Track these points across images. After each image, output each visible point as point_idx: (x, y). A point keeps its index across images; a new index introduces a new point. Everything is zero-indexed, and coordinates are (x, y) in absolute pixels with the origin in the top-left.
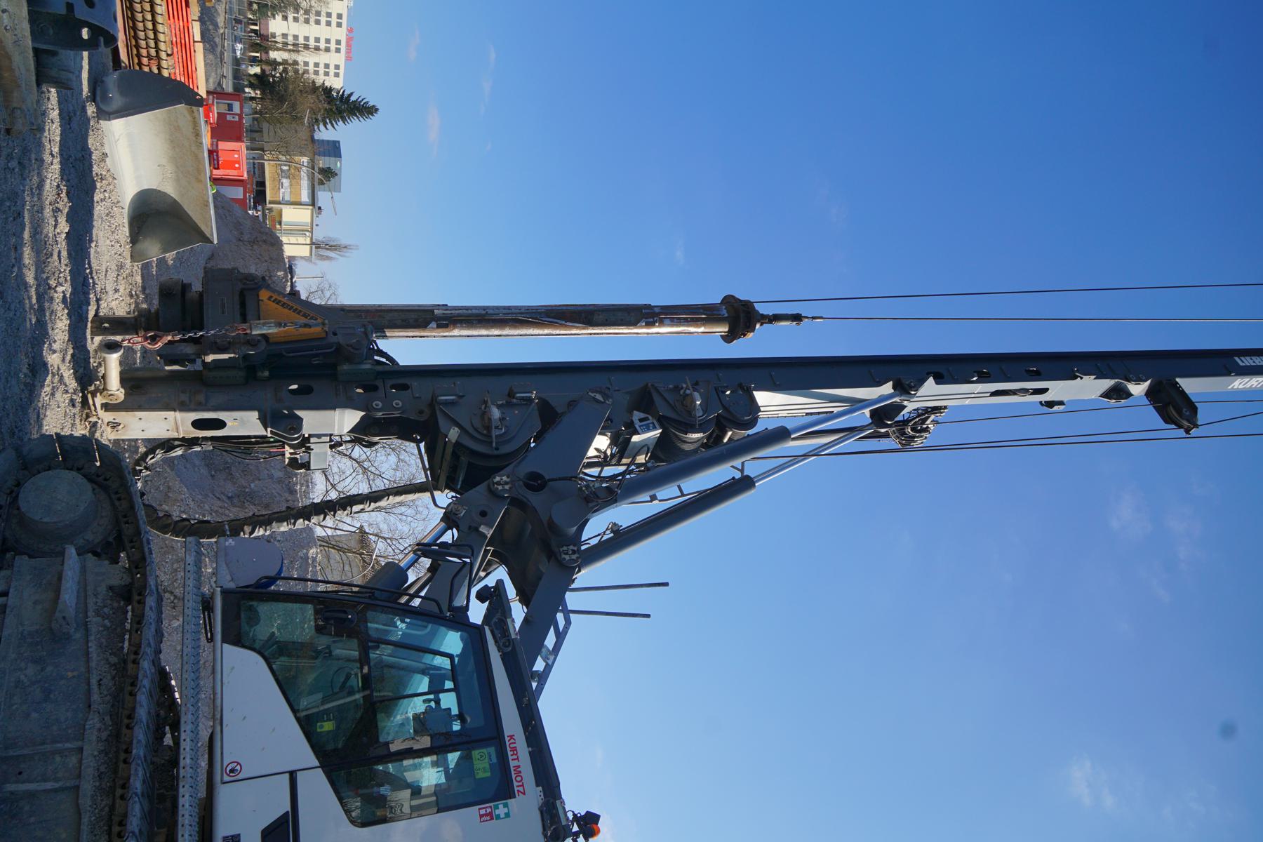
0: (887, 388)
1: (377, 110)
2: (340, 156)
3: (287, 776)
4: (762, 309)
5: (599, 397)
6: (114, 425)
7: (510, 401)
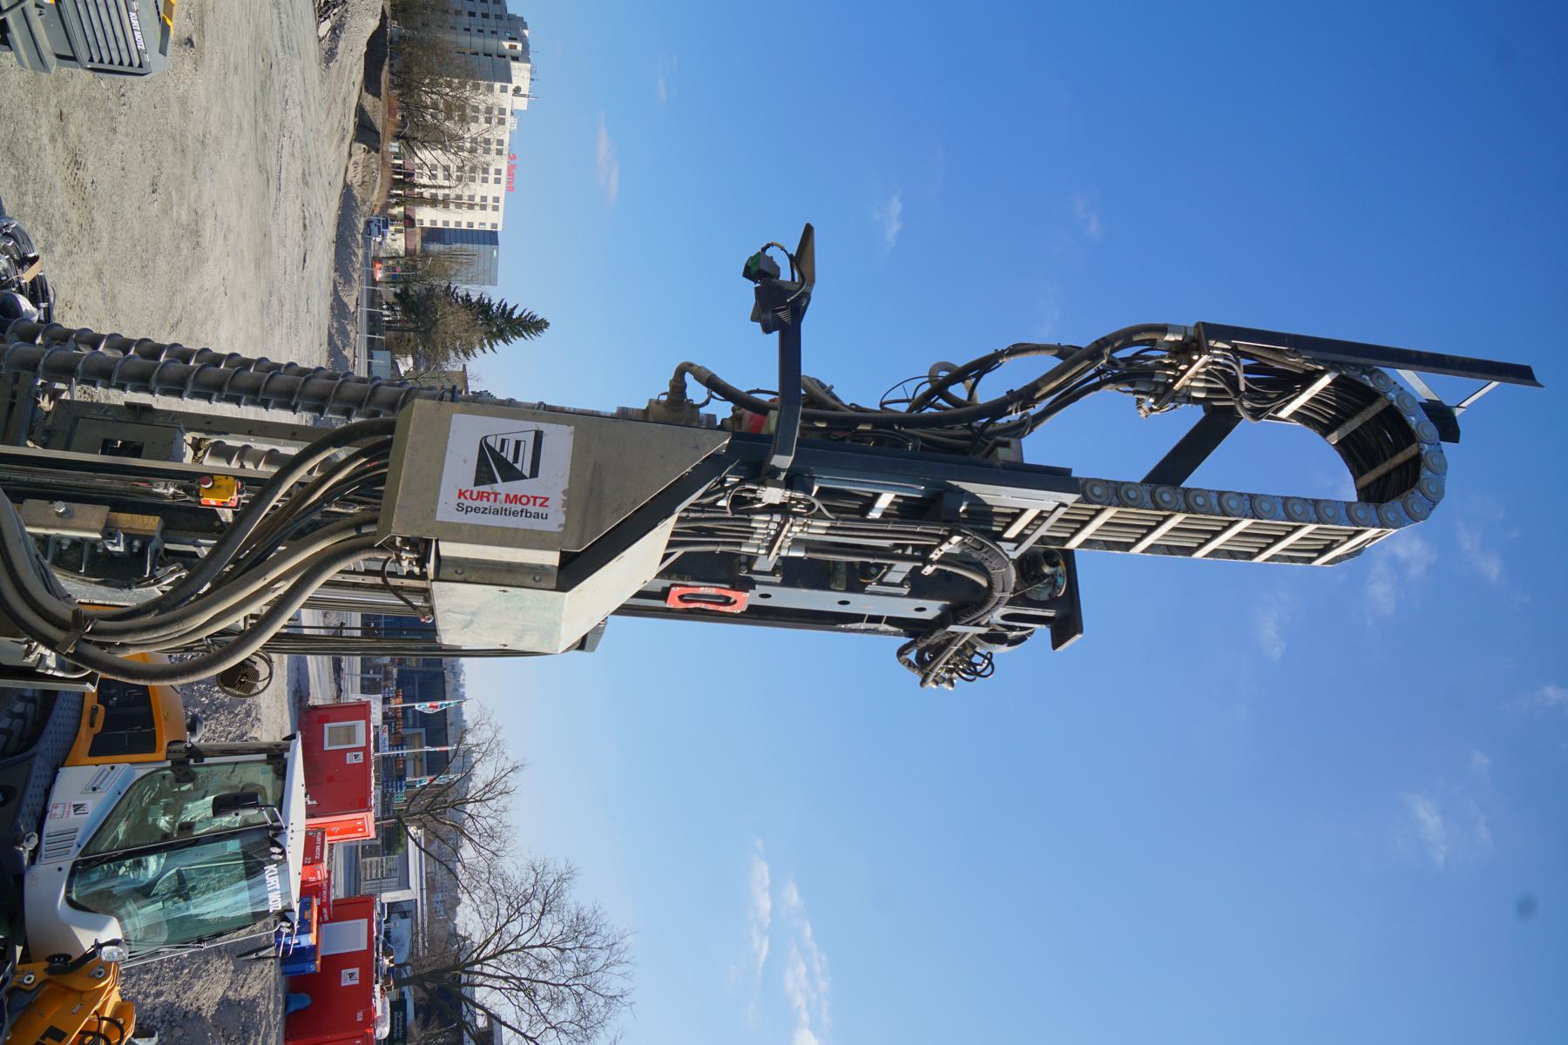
1: (547, 325)
2: (497, 244)
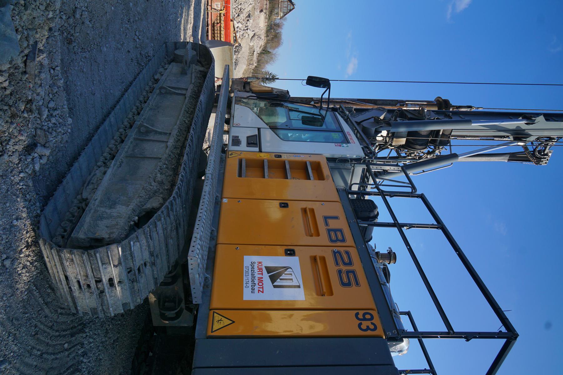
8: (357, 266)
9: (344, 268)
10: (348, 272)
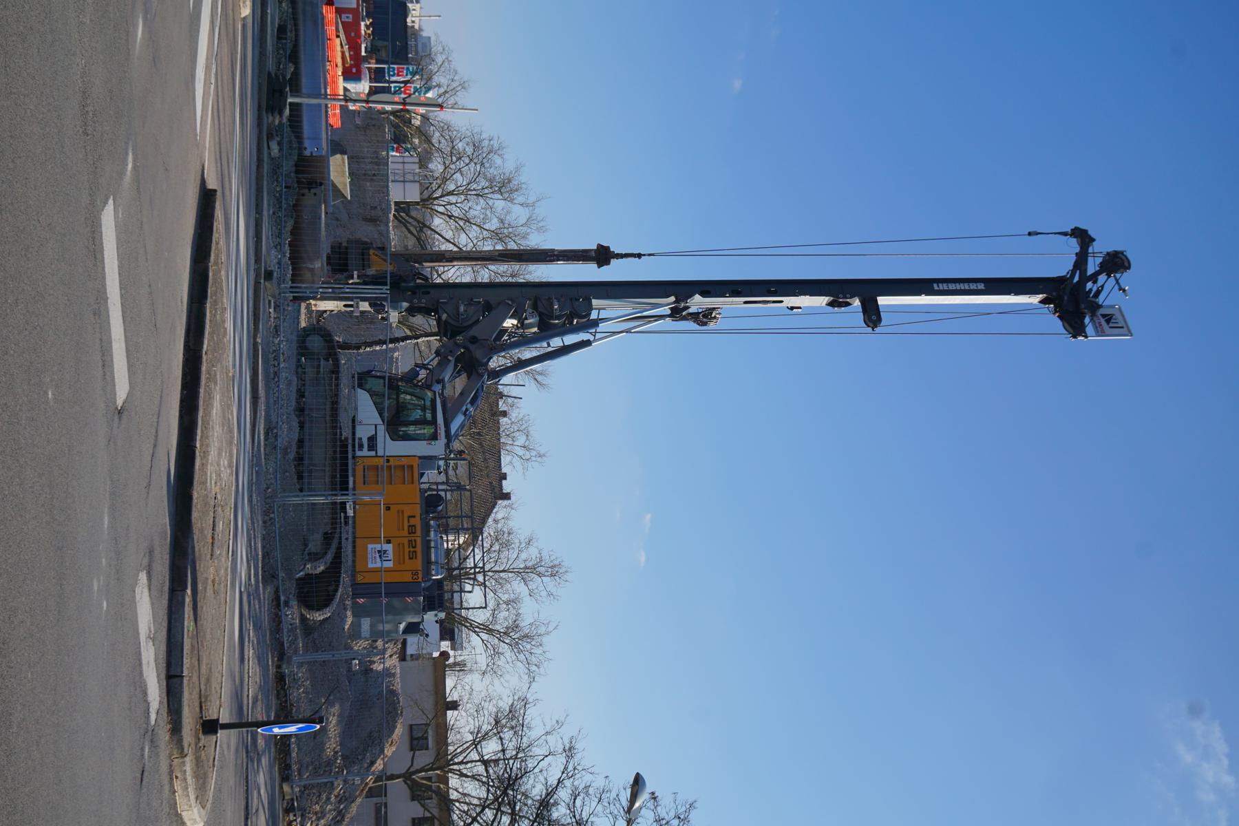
0: (672, 299)
3: (374, 426)
4: (615, 249)
5: (510, 303)
6: (315, 305)
7: (471, 302)
8: (419, 549)
9: (412, 550)
10: (413, 552)
